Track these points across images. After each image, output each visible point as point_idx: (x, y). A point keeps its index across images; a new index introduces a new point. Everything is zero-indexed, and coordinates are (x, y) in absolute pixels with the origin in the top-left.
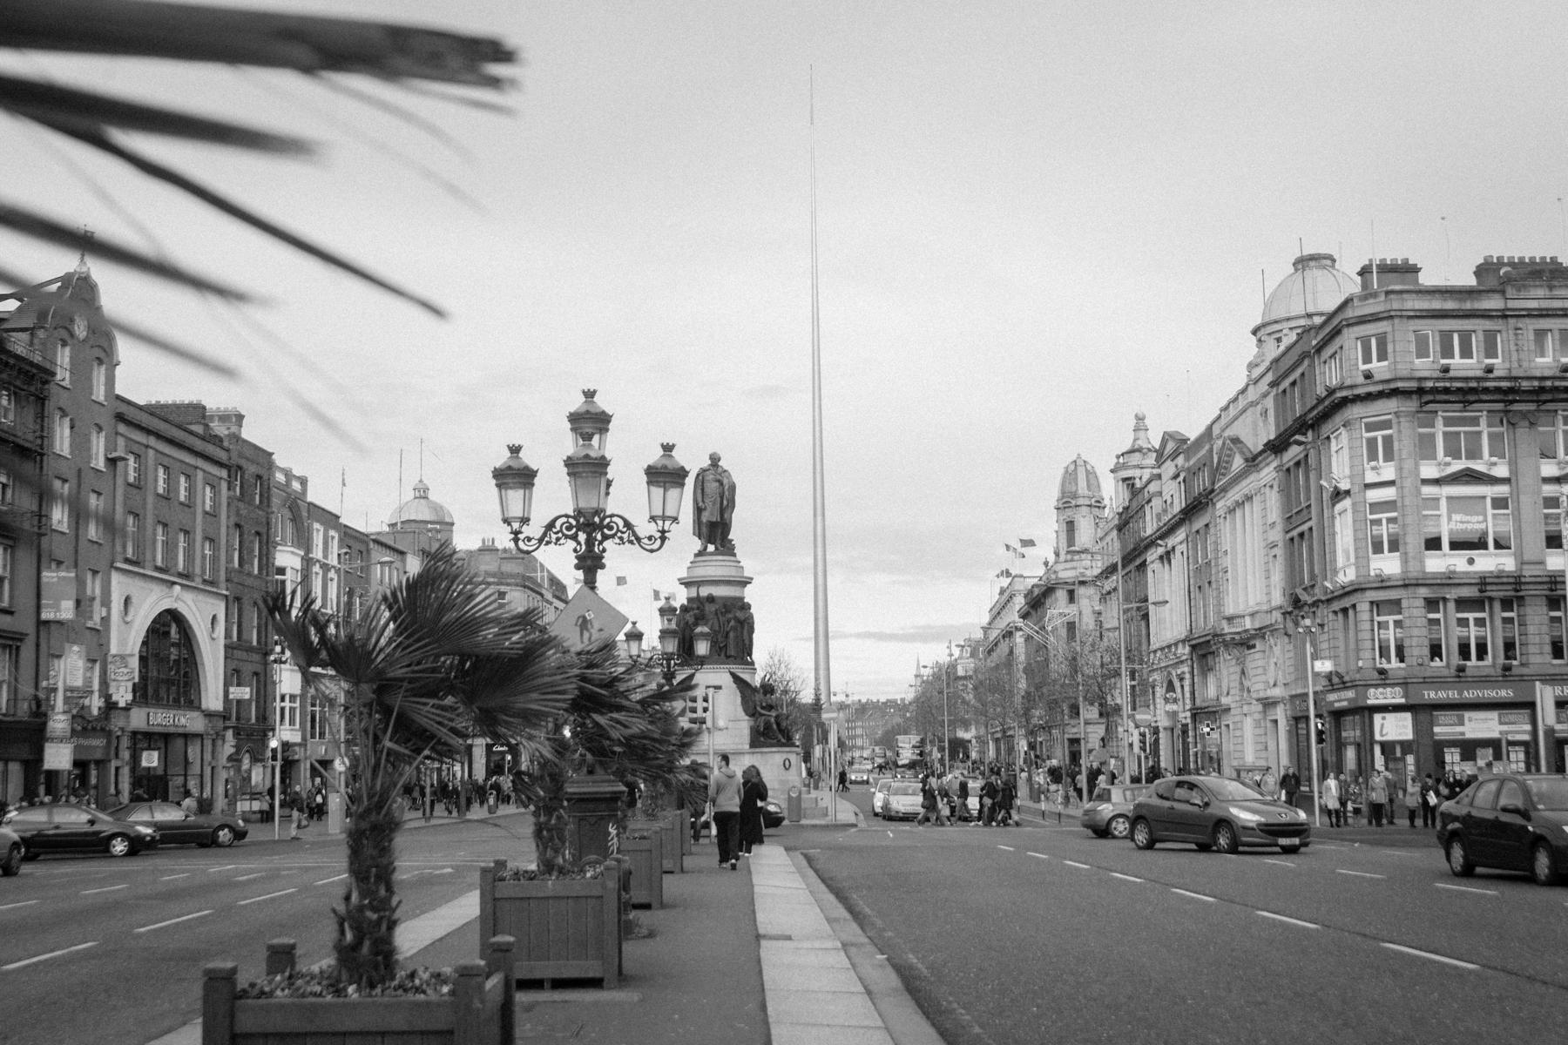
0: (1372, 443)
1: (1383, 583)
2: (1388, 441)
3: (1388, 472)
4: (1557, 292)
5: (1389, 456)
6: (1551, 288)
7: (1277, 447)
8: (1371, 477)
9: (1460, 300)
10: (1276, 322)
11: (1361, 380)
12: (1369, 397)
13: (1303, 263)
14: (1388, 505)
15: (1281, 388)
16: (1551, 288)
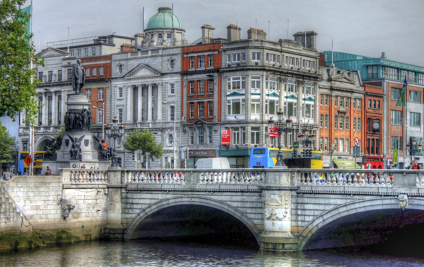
0: (253, 82)
1: (255, 122)
2: (258, 82)
3: (258, 91)
4: (290, 47)
5: (258, 86)
6: (289, 45)
7: (184, 73)
8: (253, 91)
9: (274, 45)
10: (162, 29)
11: (255, 65)
12: (257, 70)
13: (161, 10)
14: (258, 100)
15: (189, 55)
16: (289, 45)
